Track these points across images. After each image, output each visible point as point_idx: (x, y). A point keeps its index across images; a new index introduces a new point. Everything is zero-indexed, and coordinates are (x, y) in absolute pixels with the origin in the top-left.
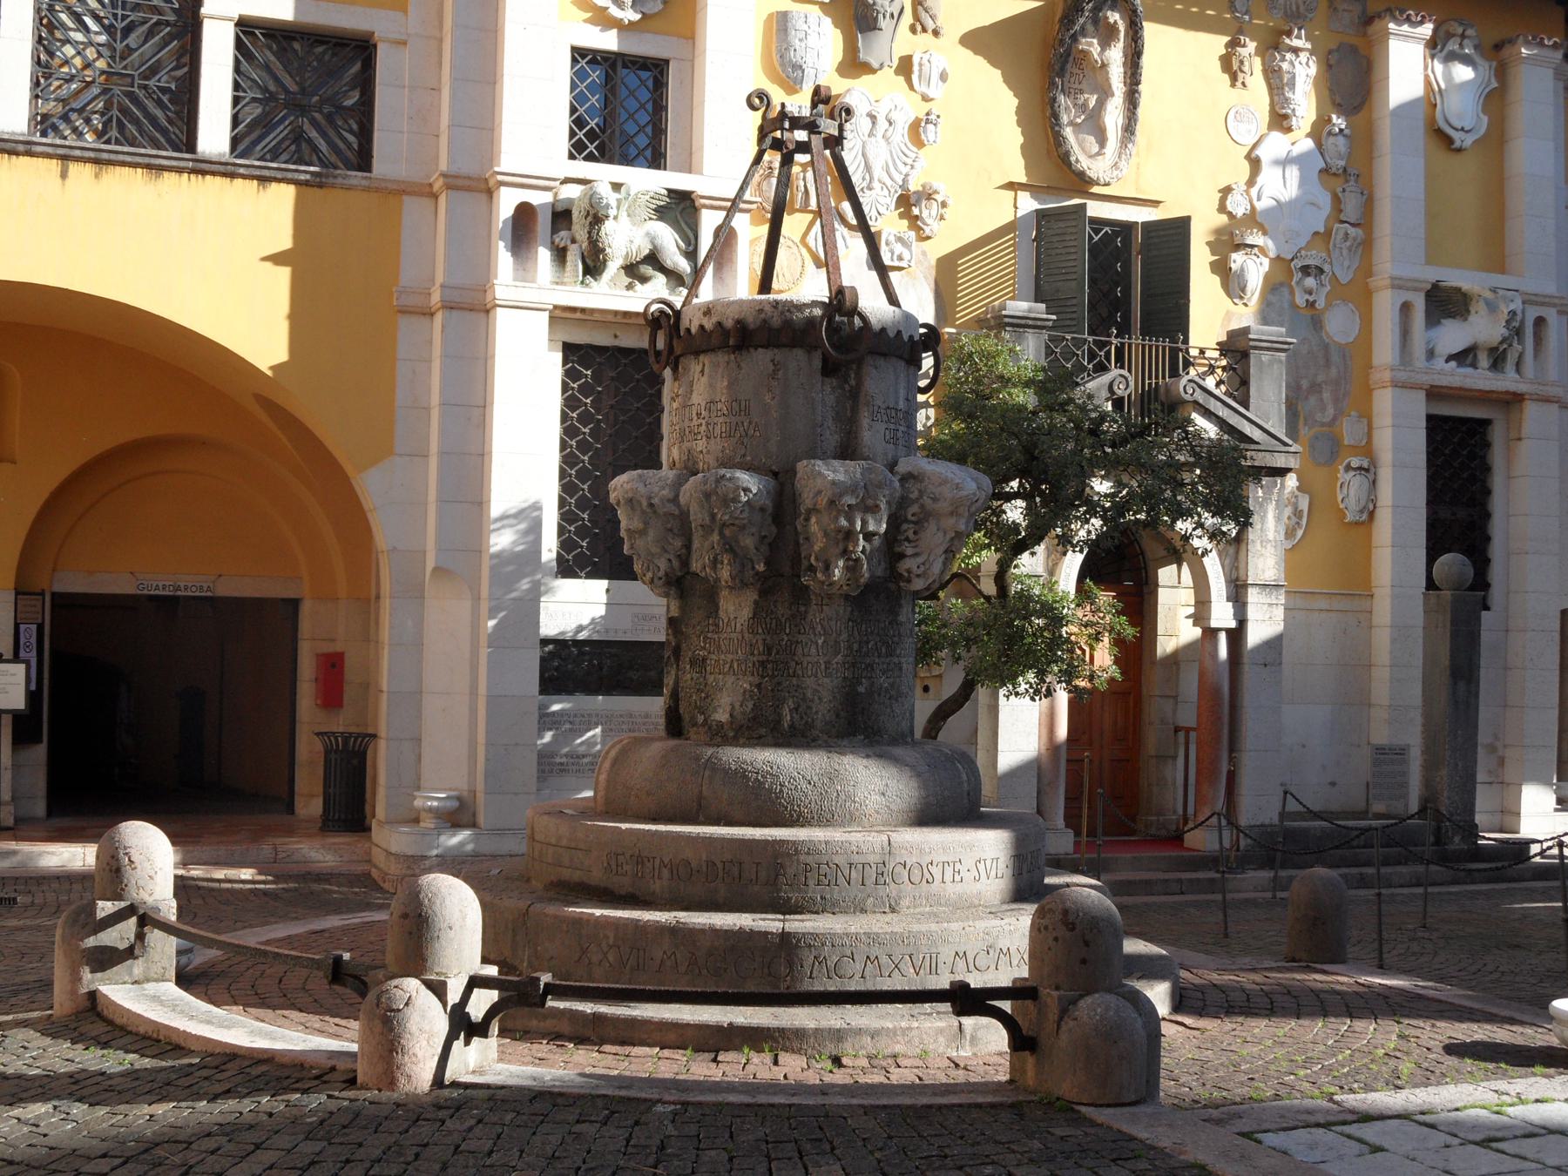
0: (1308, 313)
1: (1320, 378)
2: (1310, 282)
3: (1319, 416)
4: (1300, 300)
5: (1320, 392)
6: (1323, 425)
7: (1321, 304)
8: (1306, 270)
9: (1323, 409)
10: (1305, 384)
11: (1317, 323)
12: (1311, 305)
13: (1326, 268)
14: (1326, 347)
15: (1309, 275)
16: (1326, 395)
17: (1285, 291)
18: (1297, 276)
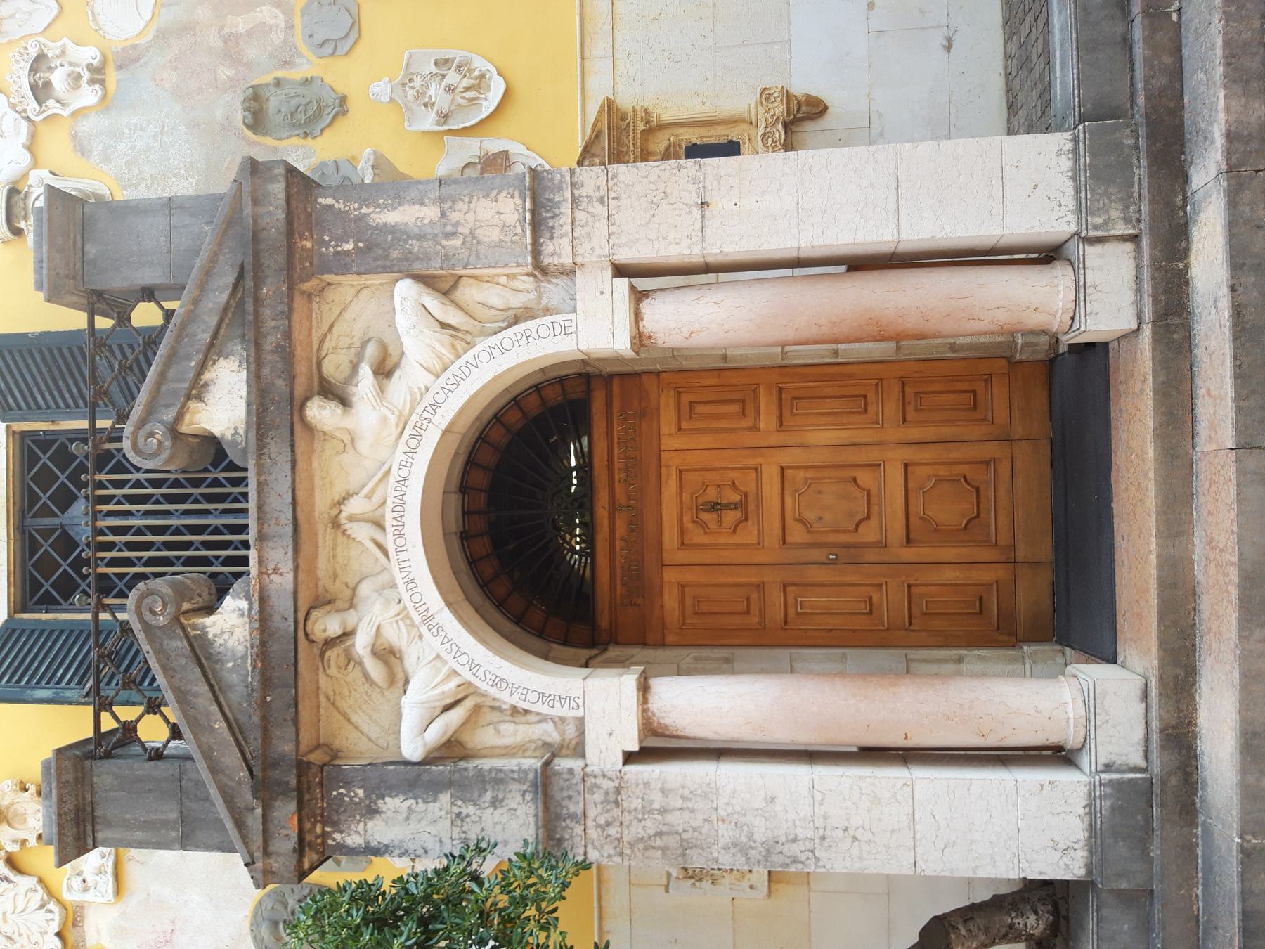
0: (112, 76)
1: (214, 41)
2: (58, 79)
3: (277, 37)
4: (88, 96)
5: (236, 36)
6: (290, 27)
7: (89, 55)
8: (41, 91)
9: (265, 29)
10: (225, 72)
11: (128, 59)
12: (97, 74)
13: (34, 52)
14: (162, 35)
15: (48, 84)
16: (240, 24)
17: (85, 126)
18: (52, 107)
